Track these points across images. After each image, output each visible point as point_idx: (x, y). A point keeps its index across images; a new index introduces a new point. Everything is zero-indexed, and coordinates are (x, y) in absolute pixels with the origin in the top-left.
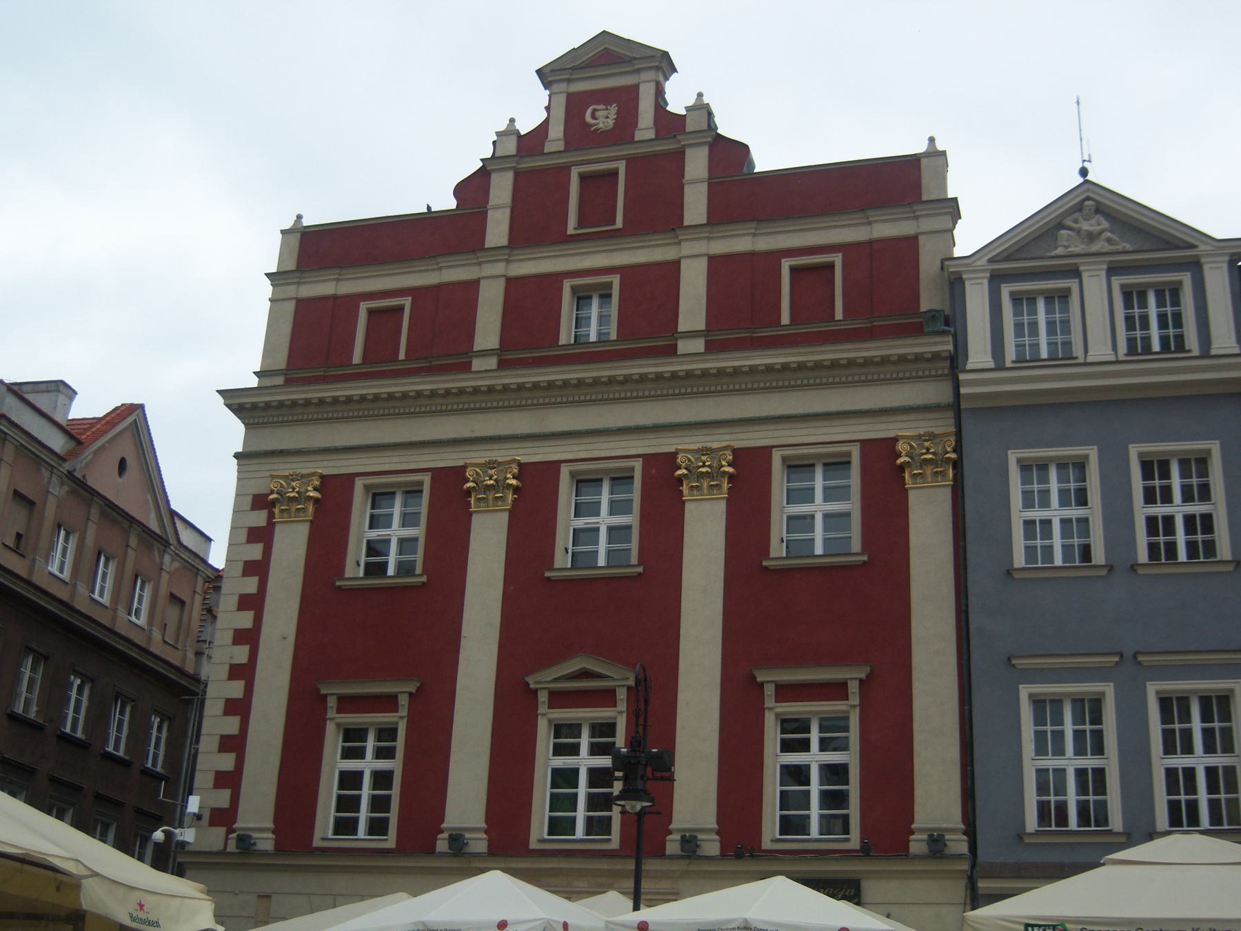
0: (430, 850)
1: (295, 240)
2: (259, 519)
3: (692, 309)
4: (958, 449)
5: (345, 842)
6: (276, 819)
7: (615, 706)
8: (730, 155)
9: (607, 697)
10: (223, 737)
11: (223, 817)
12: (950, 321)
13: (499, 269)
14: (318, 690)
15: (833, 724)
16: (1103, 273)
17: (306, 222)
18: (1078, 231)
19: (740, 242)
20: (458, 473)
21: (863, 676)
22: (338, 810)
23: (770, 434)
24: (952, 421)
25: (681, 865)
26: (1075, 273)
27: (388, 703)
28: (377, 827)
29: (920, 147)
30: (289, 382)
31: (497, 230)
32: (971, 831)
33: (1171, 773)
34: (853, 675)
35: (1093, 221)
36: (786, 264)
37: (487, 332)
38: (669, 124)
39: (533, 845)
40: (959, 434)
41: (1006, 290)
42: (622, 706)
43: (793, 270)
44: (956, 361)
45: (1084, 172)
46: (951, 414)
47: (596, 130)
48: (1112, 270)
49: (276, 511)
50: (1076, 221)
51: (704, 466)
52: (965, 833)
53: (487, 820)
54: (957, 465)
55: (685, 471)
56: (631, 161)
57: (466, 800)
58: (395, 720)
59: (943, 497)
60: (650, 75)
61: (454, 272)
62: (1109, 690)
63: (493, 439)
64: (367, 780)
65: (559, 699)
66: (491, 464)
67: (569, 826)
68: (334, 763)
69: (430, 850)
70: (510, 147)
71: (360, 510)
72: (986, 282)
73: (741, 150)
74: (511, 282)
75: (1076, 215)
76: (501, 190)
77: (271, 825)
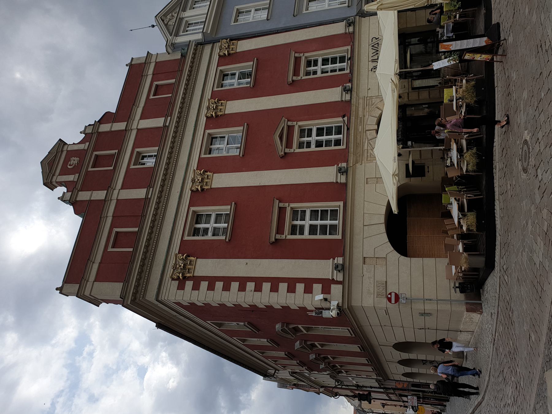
0: (345, 185)
1: (67, 286)
2: (189, 284)
8: (107, 118)
9: (290, 129)
14: (273, 242)
25: (354, 94)
26: (181, 19)
27: (282, 210)
42: (295, 123)
45: (153, 26)
57: (326, 174)
58: (289, 208)
59: (240, 42)
64: (314, 222)
65: (289, 145)
69: (345, 185)
73: (107, 114)
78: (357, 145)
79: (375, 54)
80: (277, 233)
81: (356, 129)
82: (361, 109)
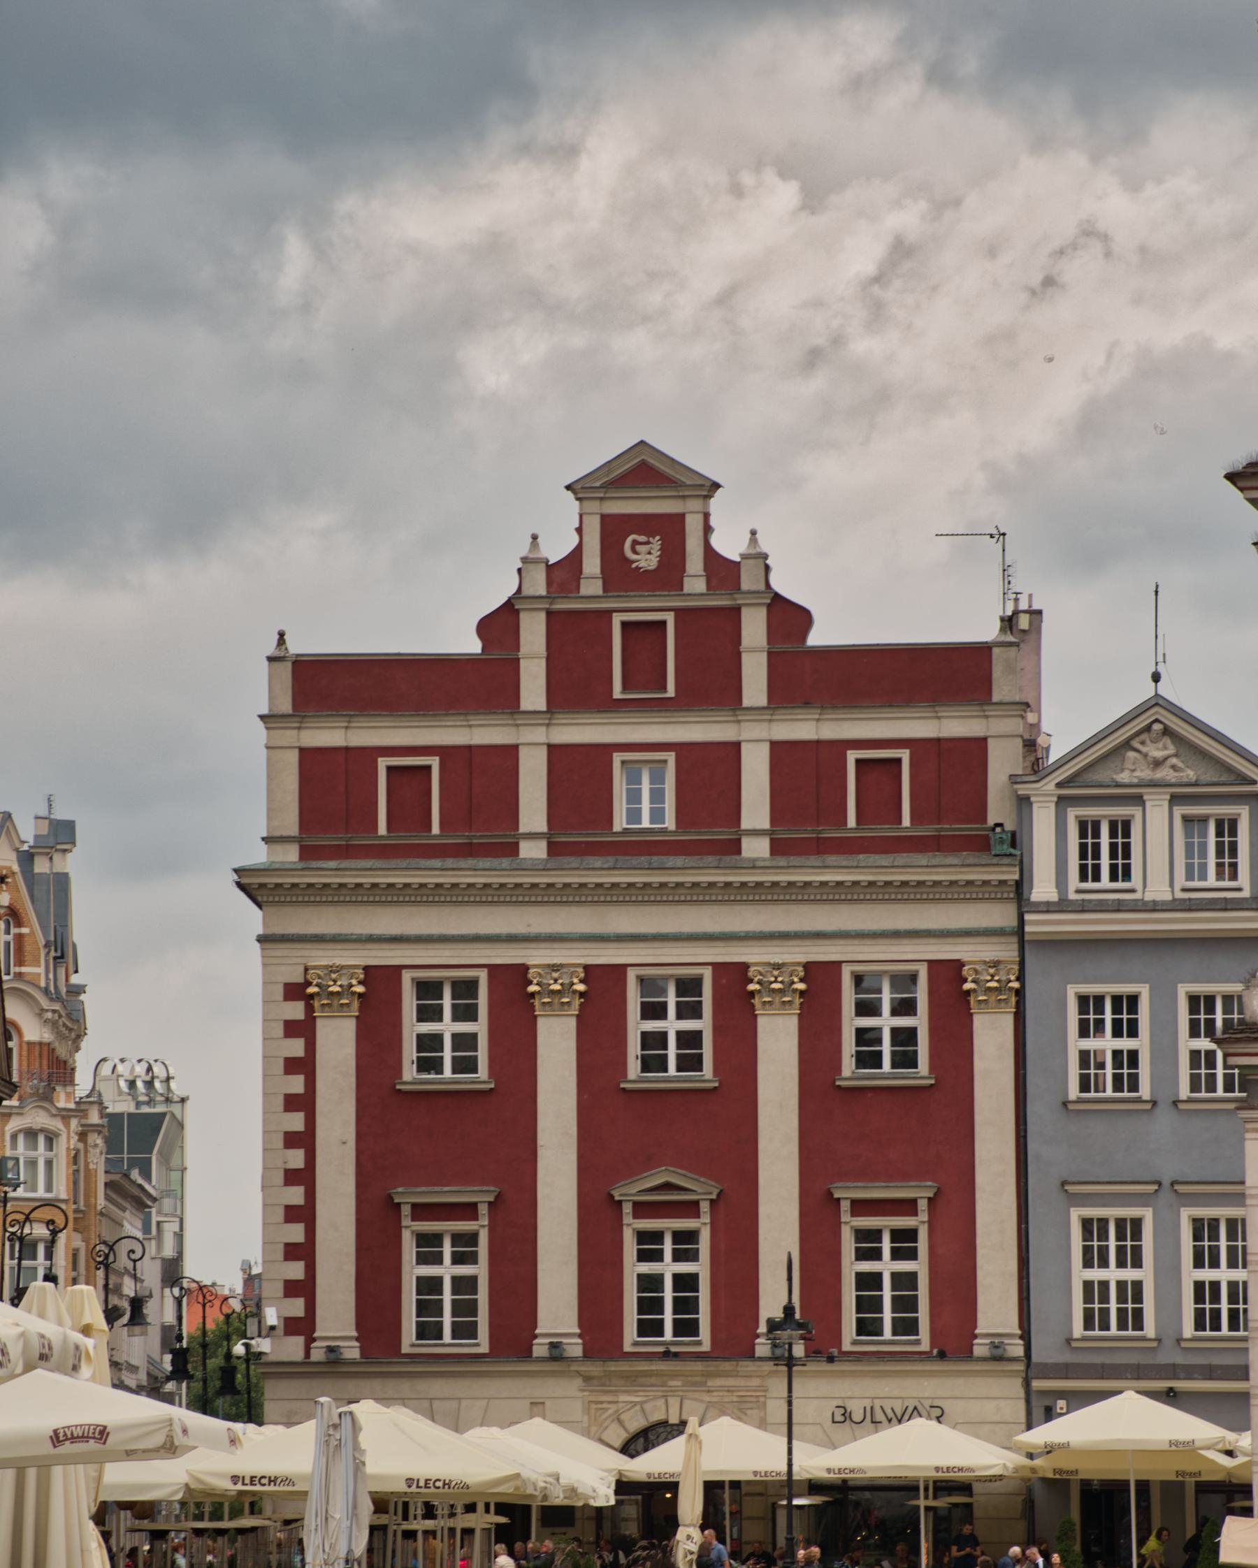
0: (525, 1353)
1: (286, 670)
2: (296, 1011)
3: (756, 809)
4: (1021, 978)
5: (429, 1347)
6: (359, 1327)
7: (699, 1217)
8: (789, 618)
9: (691, 1209)
10: (287, 1245)
11: (302, 1326)
12: (1015, 844)
13: (539, 735)
15: (904, 1237)
16: (1166, 804)
17: (297, 646)
18: (1146, 755)
19: (803, 728)
20: (521, 971)
21: (931, 1195)
22: (418, 1316)
23: (839, 948)
24: (1016, 946)
25: (769, 1366)
26: (1139, 800)
27: (469, 1211)
28: (465, 1330)
29: (988, 631)
30: (308, 853)
31: (533, 689)
32: (1026, 1336)
33: (1199, 1286)
34: (922, 1193)
35: (1160, 745)
36: (852, 756)
37: (533, 810)
38: (722, 571)
39: (627, 1347)
40: (1022, 963)
41: (1072, 814)
42: (706, 1218)
43: (859, 762)
44: (1020, 889)
45: (1156, 677)
46: (1015, 939)
47: (638, 568)
48: (1175, 800)
49: (316, 1004)
50: (1143, 743)
51: (776, 981)
52: (1021, 1337)
53: (580, 1325)
54: (1020, 993)
55: (757, 987)
56: (678, 612)
58: (476, 1228)
59: (1007, 1022)
60: (694, 505)
61: (485, 733)
62: (1147, 1215)
63: (558, 939)
65: (642, 1209)
66: (555, 968)
67: (658, 1328)
68: (412, 1271)
70: (538, 584)
71: (409, 1002)
72: (1053, 806)
74: (554, 750)
75: (1144, 736)
76: (533, 632)
77: (355, 1334)
78: (632, 1379)
79: (890, 1414)
80: (415, 1206)
81: (674, 1375)
82: (730, 1382)
